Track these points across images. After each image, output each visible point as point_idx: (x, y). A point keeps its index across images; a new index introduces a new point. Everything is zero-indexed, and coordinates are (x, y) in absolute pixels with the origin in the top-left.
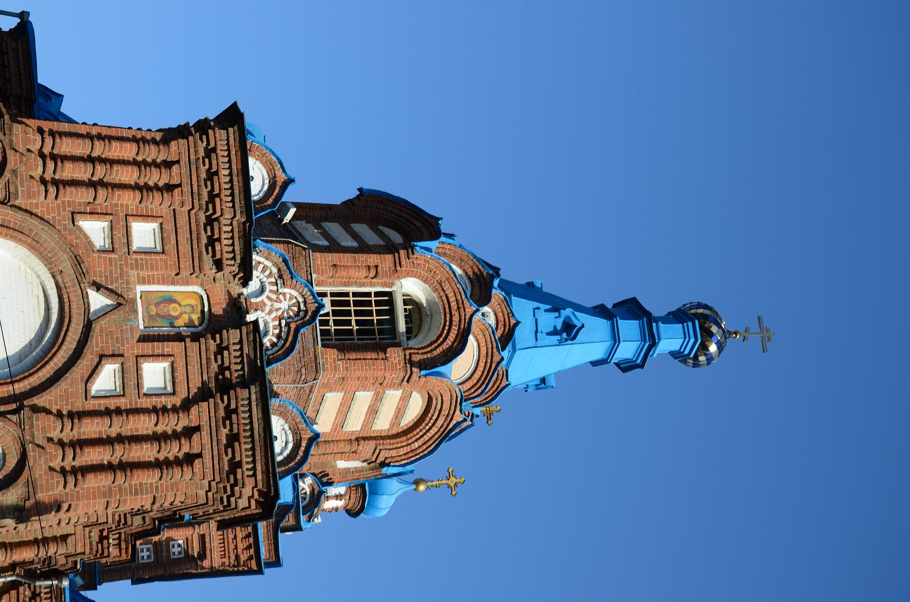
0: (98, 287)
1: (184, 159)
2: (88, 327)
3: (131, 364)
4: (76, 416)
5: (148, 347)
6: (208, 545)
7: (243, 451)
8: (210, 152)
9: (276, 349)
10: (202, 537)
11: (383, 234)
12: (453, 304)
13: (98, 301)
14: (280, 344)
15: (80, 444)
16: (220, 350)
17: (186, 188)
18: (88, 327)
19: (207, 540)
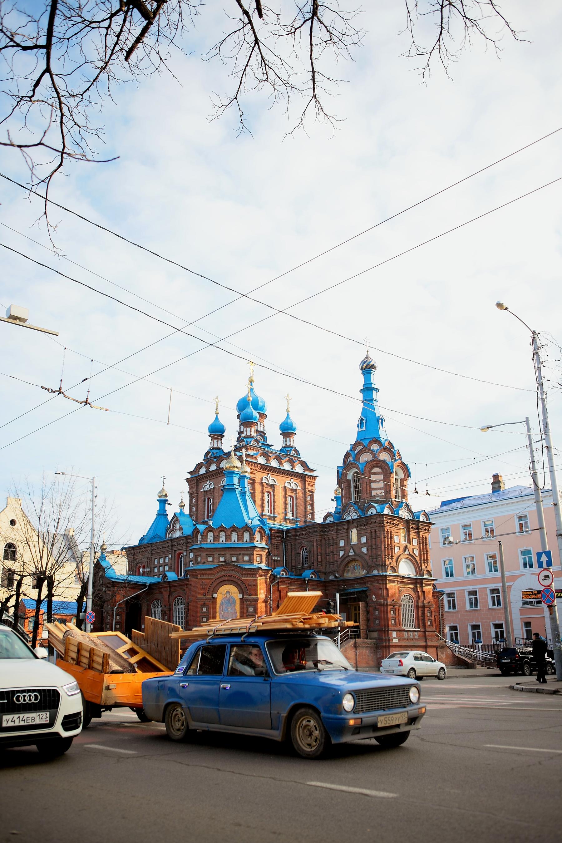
0: (405, 551)
1: (387, 528)
2: (410, 555)
3: (414, 547)
4: (421, 560)
5: (411, 543)
6: (311, 490)
7: (427, 528)
8: (387, 523)
9: (411, 514)
10: (309, 491)
11: (375, 472)
12: (398, 464)
13: (407, 552)
14: (410, 513)
15: (424, 559)
16: (412, 528)
17: (392, 529)
18: (410, 555)
19: (309, 490)
